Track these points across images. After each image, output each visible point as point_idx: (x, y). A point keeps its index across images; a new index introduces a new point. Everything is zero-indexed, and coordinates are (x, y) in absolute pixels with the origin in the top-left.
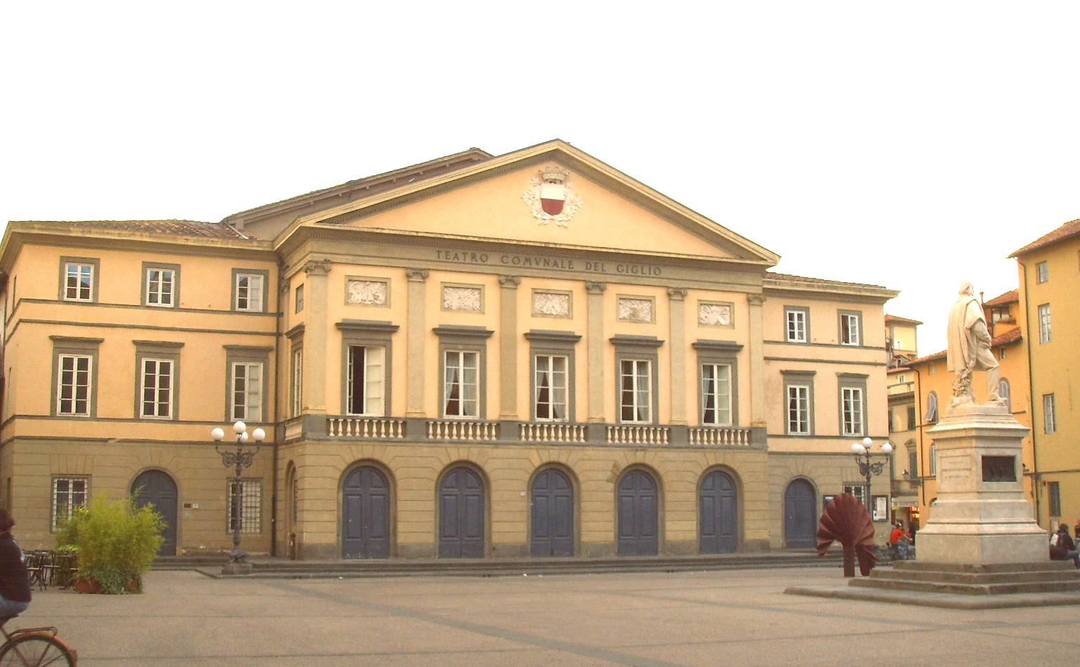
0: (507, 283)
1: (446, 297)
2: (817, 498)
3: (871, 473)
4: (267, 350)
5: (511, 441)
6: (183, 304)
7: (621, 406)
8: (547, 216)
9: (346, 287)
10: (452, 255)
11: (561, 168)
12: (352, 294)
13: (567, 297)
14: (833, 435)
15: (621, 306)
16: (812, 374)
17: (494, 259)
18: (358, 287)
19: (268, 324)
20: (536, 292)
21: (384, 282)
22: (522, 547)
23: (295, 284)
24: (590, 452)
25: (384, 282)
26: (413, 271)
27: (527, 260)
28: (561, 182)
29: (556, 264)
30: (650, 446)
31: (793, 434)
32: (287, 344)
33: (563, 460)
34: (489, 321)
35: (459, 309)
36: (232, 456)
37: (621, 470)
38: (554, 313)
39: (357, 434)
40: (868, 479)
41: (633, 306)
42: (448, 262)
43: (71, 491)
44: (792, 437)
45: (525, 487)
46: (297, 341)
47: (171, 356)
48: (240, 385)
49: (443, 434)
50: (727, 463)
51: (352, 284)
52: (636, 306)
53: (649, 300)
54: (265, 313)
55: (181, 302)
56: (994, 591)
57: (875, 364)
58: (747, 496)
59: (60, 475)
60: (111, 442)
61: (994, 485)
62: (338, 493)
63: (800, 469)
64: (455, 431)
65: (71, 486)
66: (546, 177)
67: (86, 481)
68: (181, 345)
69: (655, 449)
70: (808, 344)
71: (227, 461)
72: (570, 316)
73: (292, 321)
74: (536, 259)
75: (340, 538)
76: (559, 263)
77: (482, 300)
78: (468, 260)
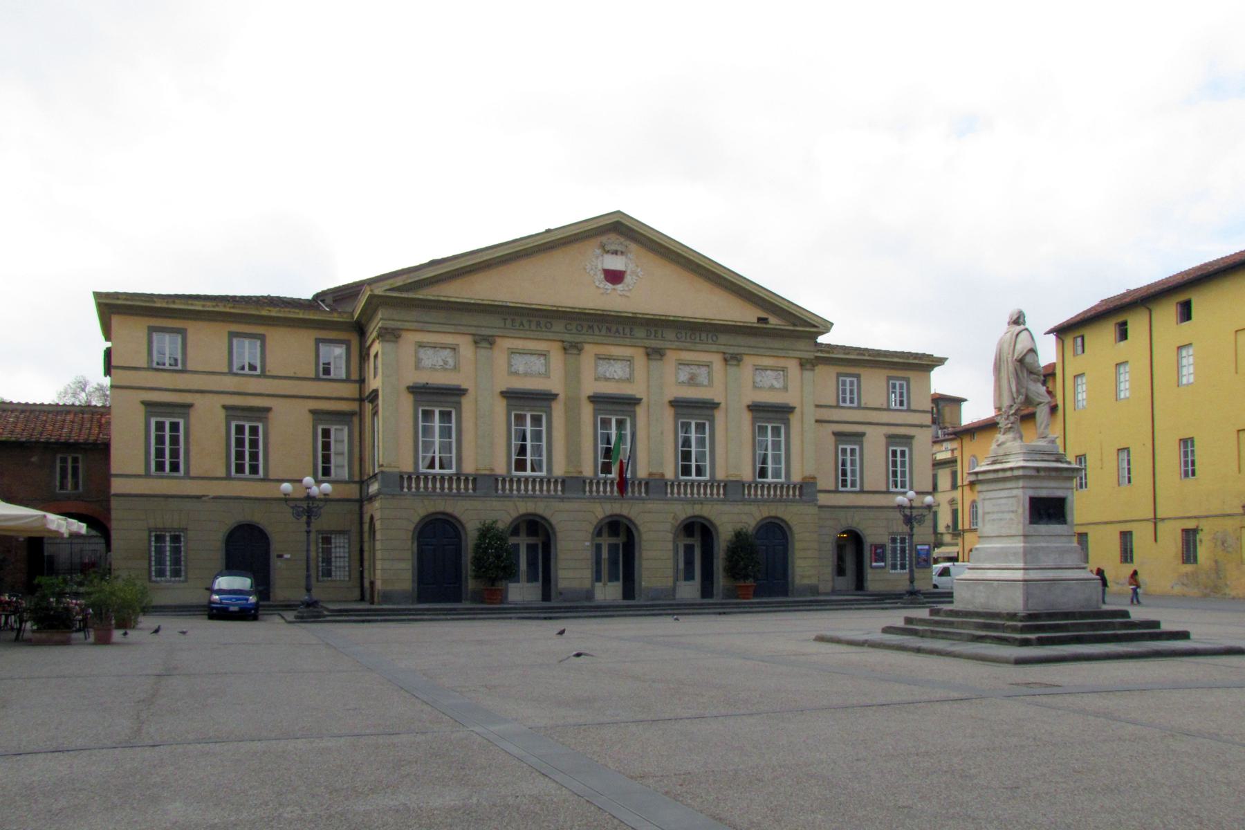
0: (572, 348)
1: (513, 362)
3: (915, 524)
4: (351, 414)
5: (575, 496)
6: (269, 371)
8: (609, 286)
9: (416, 352)
10: (517, 324)
11: (622, 240)
12: (422, 359)
13: (628, 363)
15: (680, 371)
16: (862, 435)
17: (559, 326)
18: (428, 352)
19: (350, 390)
23: (373, 352)
24: (651, 506)
25: (454, 349)
26: (481, 337)
27: (591, 327)
28: (622, 253)
29: (617, 331)
30: (707, 500)
31: (844, 489)
32: (368, 407)
33: (625, 512)
34: (554, 384)
35: (526, 374)
36: (301, 509)
37: (679, 522)
38: (617, 377)
39: (430, 489)
40: (912, 529)
41: (691, 371)
42: (514, 329)
43: (168, 544)
44: (842, 492)
46: (375, 404)
47: (259, 419)
48: (326, 446)
49: (511, 490)
50: (779, 515)
51: (422, 351)
52: (694, 371)
53: (708, 365)
54: (348, 380)
55: (267, 369)
56: (1042, 642)
57: (922, 426)
58: (798, 545)
59: (156, 529)
60: (204, 498)
61: (1043, 528)
62: (413, 543)
64: (522, 487)
66: (608, 248)
67: (182, 534)
68: (268, 410)
69: (712, 503)
70: (859, 408)
71: (298, 515)
72: (632, 380)
73: (374, 383)
74: (598, 327)
76: (621, 331)
77: (547, 364)
78: (533, 327)
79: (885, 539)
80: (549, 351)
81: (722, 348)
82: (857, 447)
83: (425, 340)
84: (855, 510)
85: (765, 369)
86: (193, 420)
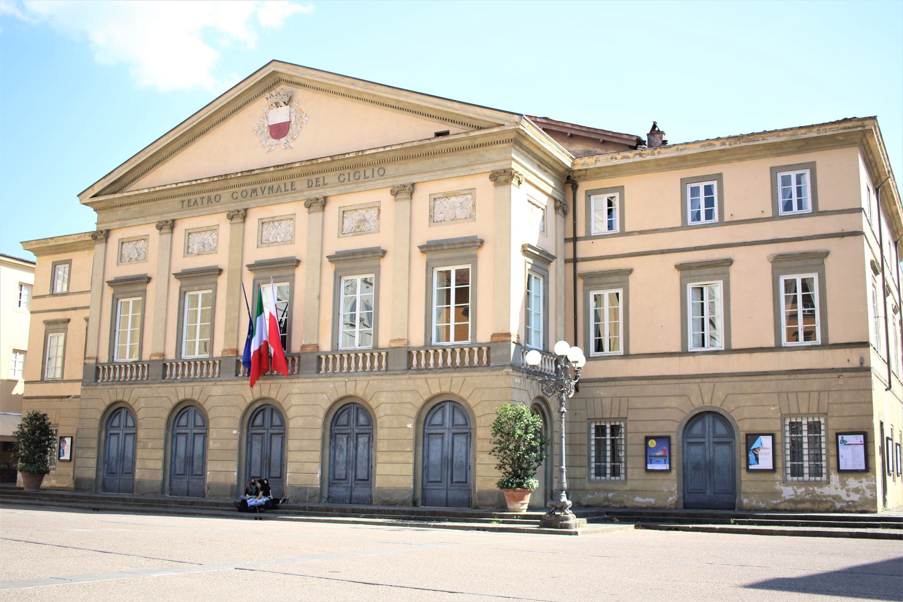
13: (292, 222)
16: (729, 262)
17: (226, 195)
22: (232, 486)
29: (279, 188)
33: (273, 395)
34: (220, 259)
38: (279, 240)
45: (237, 423)
63: (707, 399)
79: (775, 426)
81: (391, 182)
85: (447, 196)
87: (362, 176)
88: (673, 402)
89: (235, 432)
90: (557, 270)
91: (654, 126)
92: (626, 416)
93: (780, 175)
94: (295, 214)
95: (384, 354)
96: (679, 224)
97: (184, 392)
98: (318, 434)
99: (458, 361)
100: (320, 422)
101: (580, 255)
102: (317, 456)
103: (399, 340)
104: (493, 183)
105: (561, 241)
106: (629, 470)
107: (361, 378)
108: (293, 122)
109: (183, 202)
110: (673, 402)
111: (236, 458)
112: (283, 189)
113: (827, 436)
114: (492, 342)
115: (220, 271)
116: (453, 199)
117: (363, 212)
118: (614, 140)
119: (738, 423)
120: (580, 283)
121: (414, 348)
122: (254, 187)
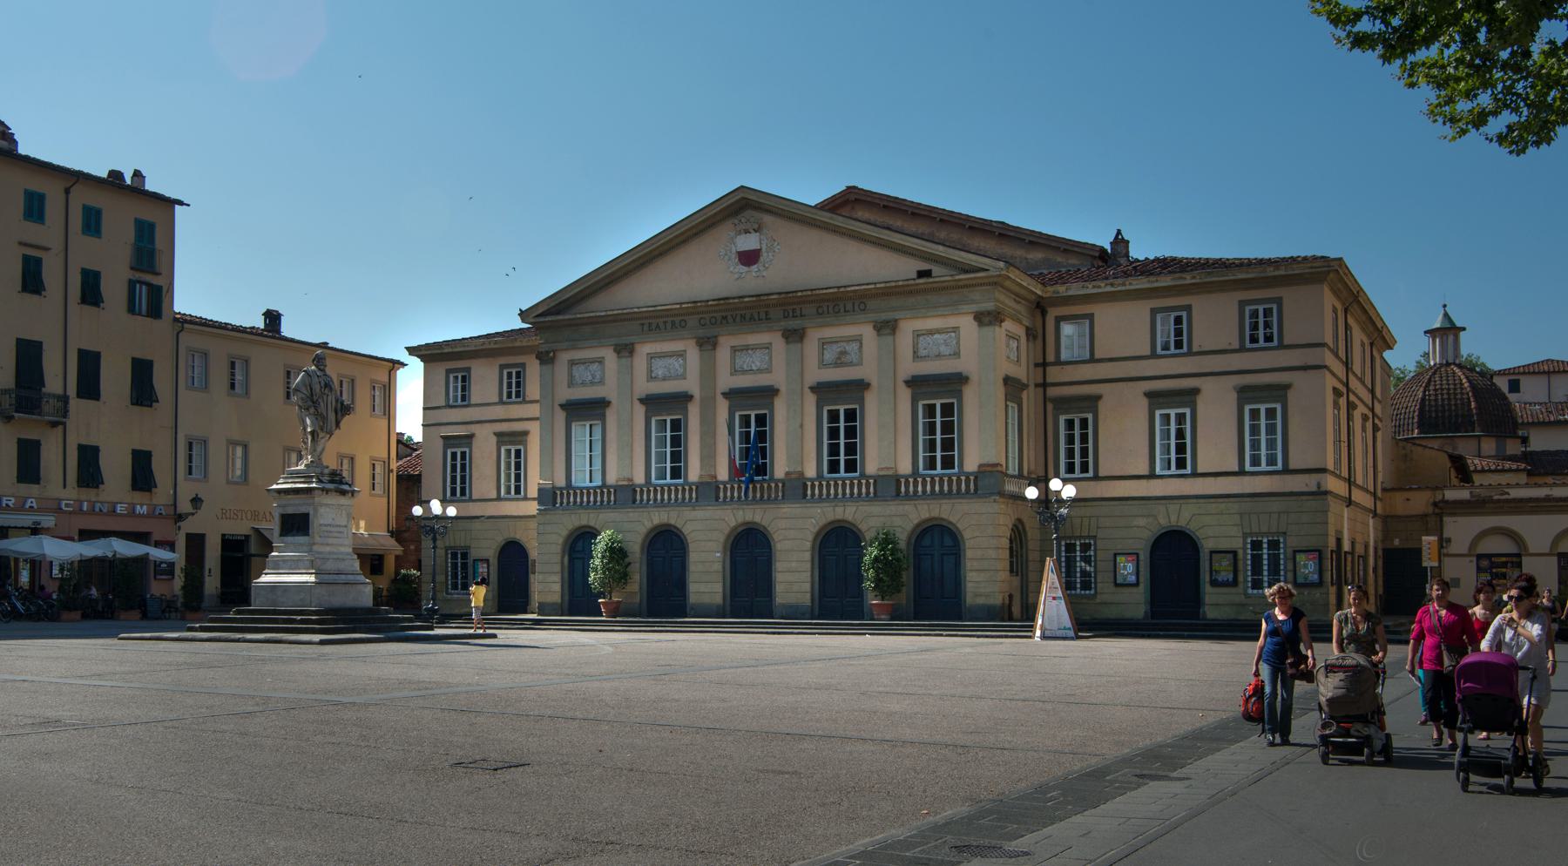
2: (1201, 554)
7: (858, 457)
8: (744, 269)
14: (386, 502)
20: (734, 350)
21: (600, 361)
28: (756, 231)
33: (757, 519)
34: (691, 385)
36: (429, 528)
38: (754, 368)
45: (721, 548)
47: (520, 443)
51: (574, 368)
58: (969, 554)
59: (451, 548)
60: (483, 519)
62: (563, 557)
63: (1173, 519)
65: (1265, 546)
75: (567, 598)
79: (1236, 544)
80: (685, 351)
82: (1187, 411)
83: (576, 358)
84: (1181, 501)
85: (931, 332)
86: (474, 450)
87: (842, 310)
88: (1141, 522)
89: (718, 555)
90: (1029, 397)
91: (1119, 232)
92: (1095, 534)
93: (1248, 309)
94: (771, 344)
95: (872, 481)
96: (1148, 353)
97: (658, 517)
98: (808, 556)
99: (946, 488)
100: (808, 545)
101: (1049, 380)
102: (807, 576)
103: (888, 468)
104: (976, 323)
105: (1032, 366)
106: (1099, 585)
107: (849, 504)
108: (764, 250)
109: (643, 324)
110: (1141, 522)
111: (721, 579)
112: (756, 317)
113: (1285, 553)
114: (979, 472)
115: (691, 397)
116: (936, 336)
117: (845, 344)
118: (1076, 249)
119: (1203, 541)
120: (1050, 407)
121: (902, 476)
122: (724, 314)
